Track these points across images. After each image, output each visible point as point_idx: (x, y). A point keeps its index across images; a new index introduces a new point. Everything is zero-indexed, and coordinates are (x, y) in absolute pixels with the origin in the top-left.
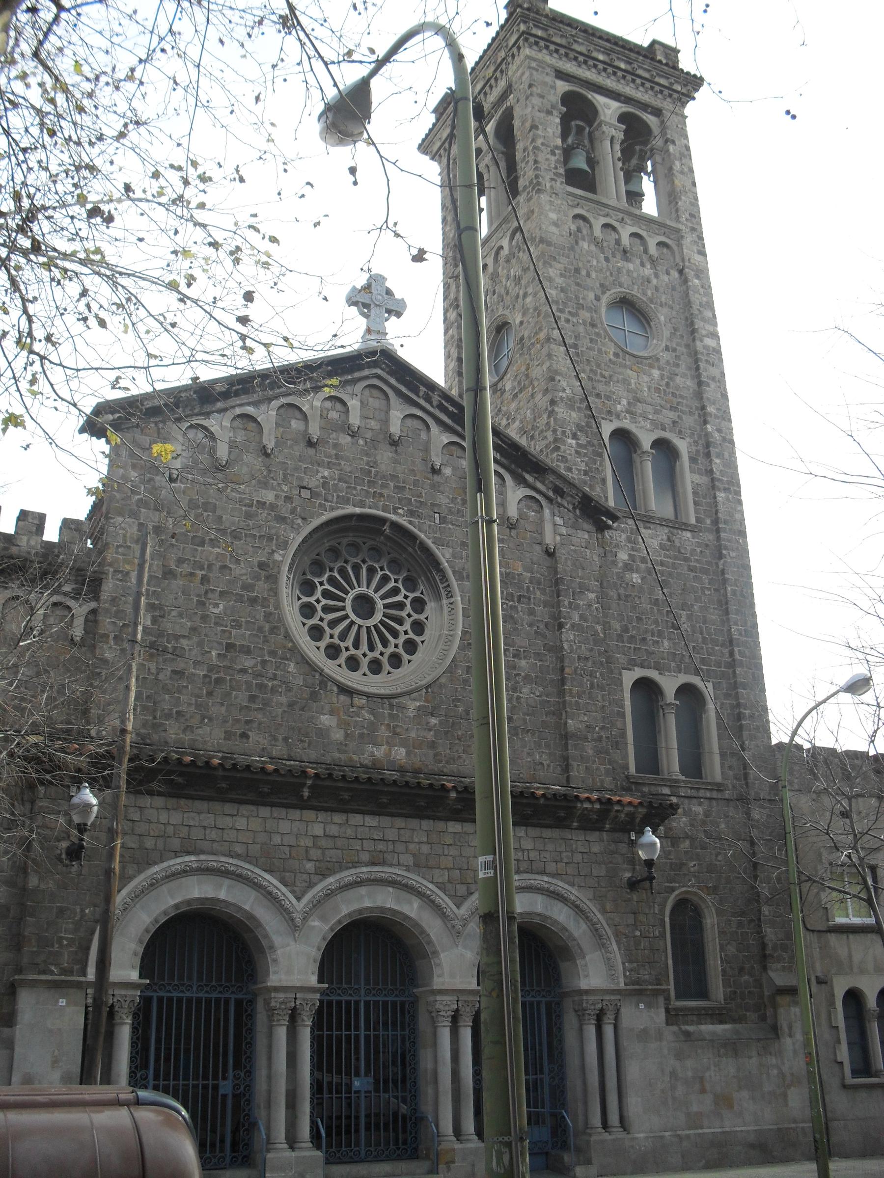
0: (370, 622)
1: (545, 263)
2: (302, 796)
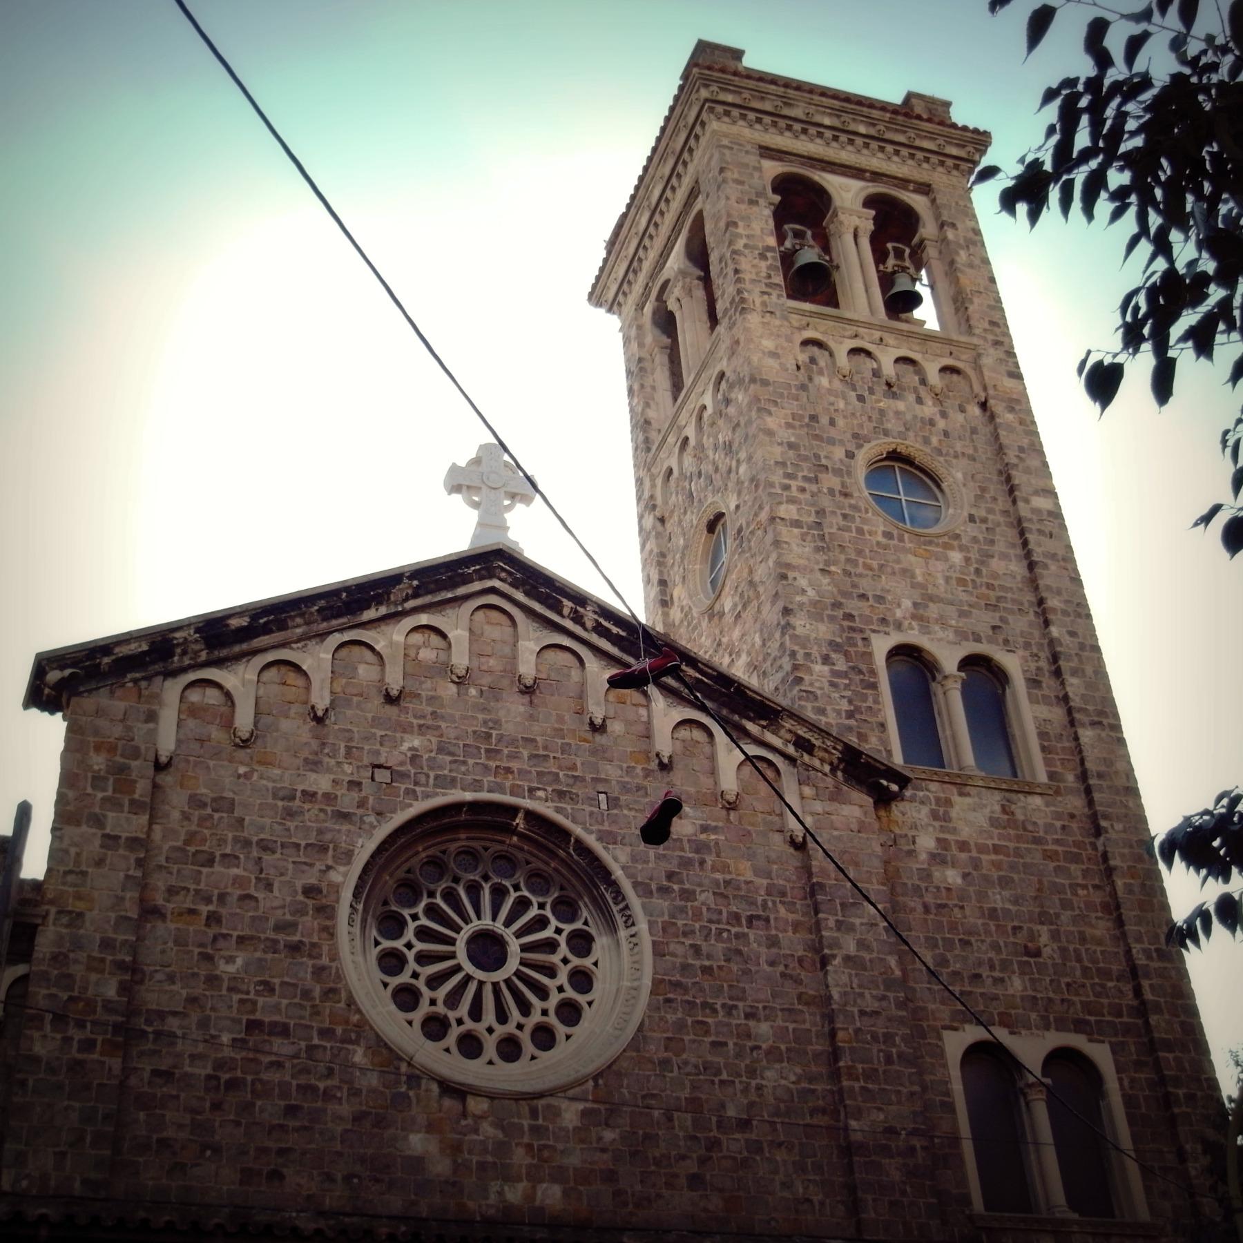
1: (759, 410)
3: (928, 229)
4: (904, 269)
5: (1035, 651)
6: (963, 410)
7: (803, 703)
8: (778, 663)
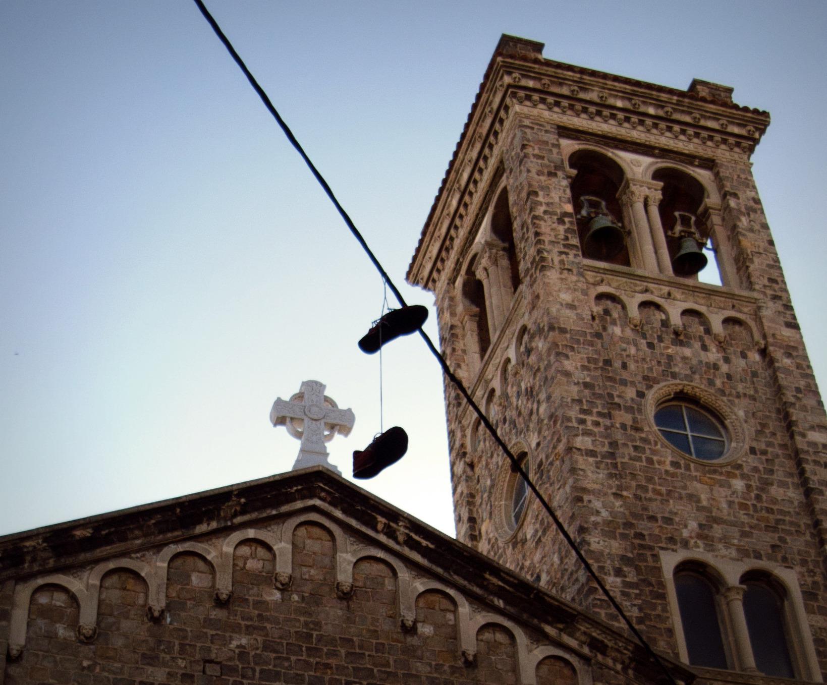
3: (713, 199)
4: (691, 234)
5: (811, 567)
6: (744, 356)
7: (597, 610)
8: (575, 576)
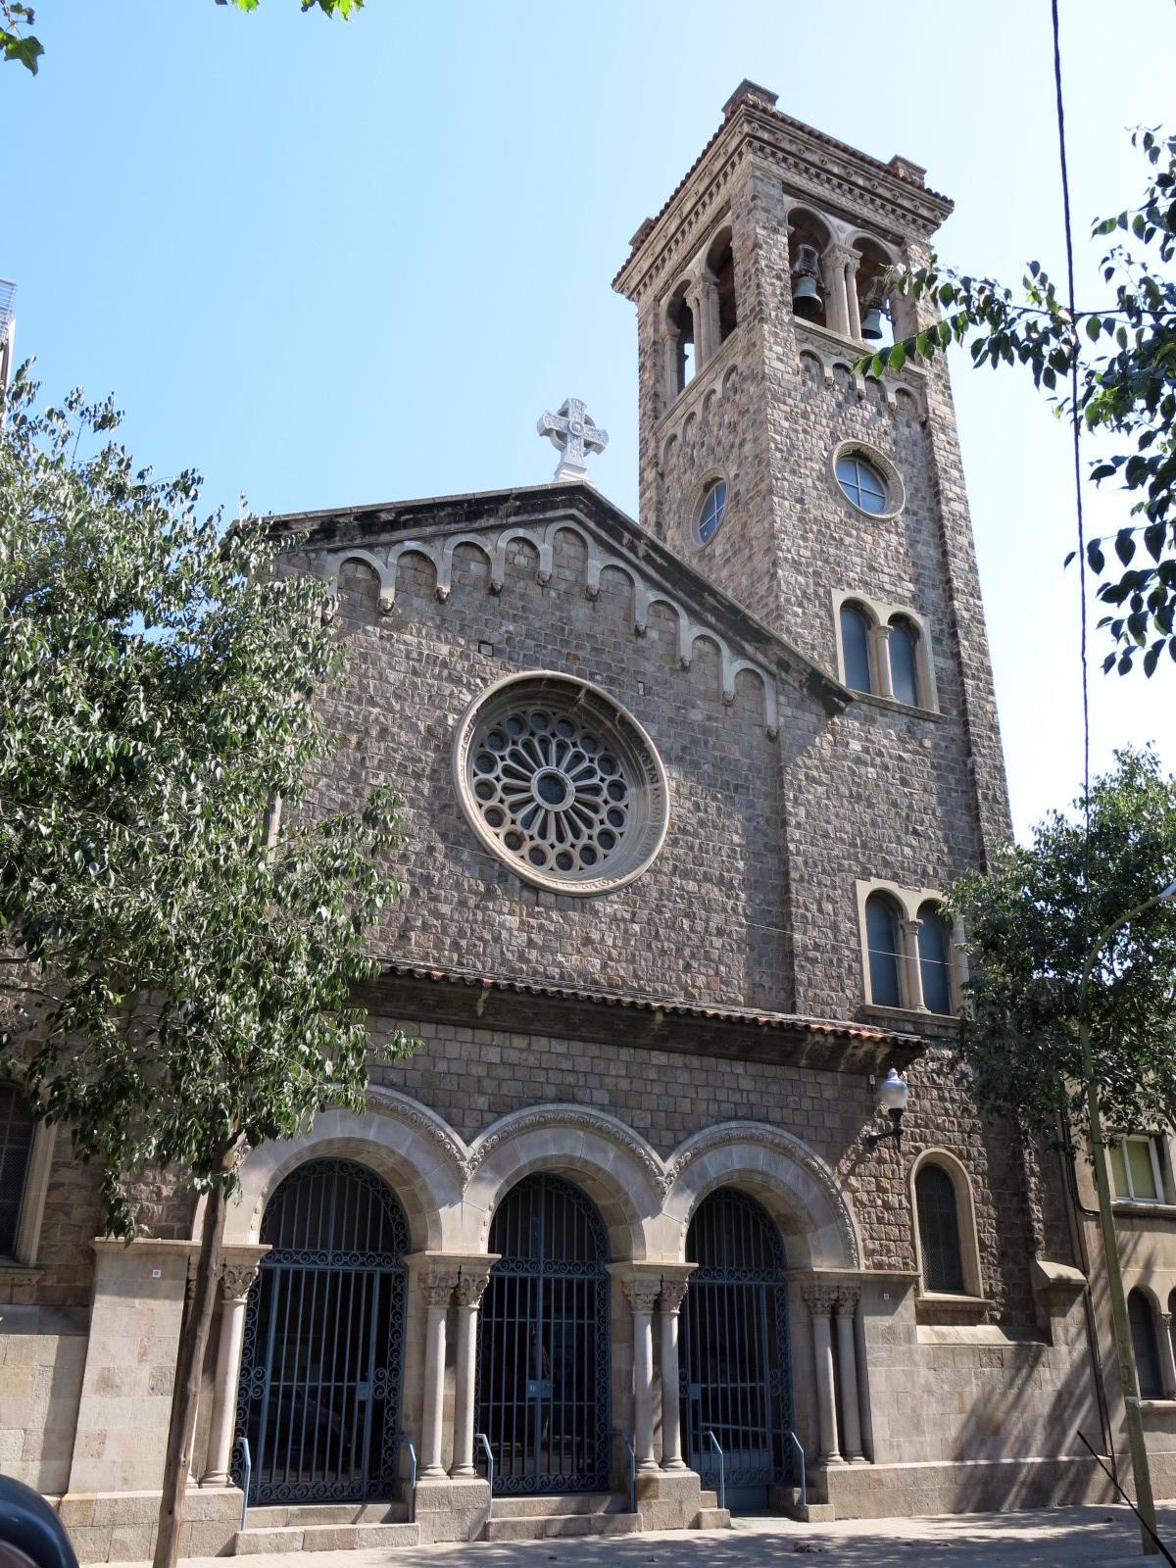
0: (560, 808)
2: (475, 1012)
